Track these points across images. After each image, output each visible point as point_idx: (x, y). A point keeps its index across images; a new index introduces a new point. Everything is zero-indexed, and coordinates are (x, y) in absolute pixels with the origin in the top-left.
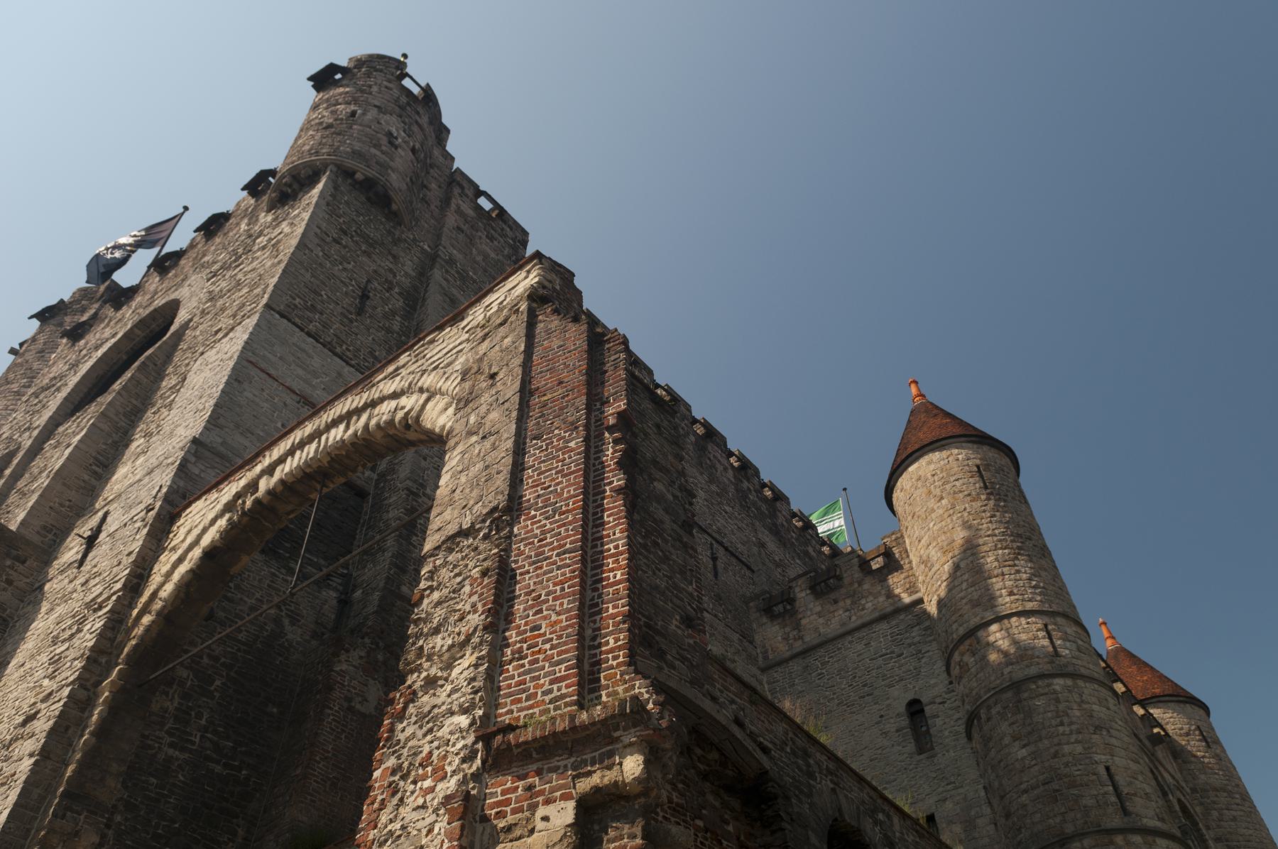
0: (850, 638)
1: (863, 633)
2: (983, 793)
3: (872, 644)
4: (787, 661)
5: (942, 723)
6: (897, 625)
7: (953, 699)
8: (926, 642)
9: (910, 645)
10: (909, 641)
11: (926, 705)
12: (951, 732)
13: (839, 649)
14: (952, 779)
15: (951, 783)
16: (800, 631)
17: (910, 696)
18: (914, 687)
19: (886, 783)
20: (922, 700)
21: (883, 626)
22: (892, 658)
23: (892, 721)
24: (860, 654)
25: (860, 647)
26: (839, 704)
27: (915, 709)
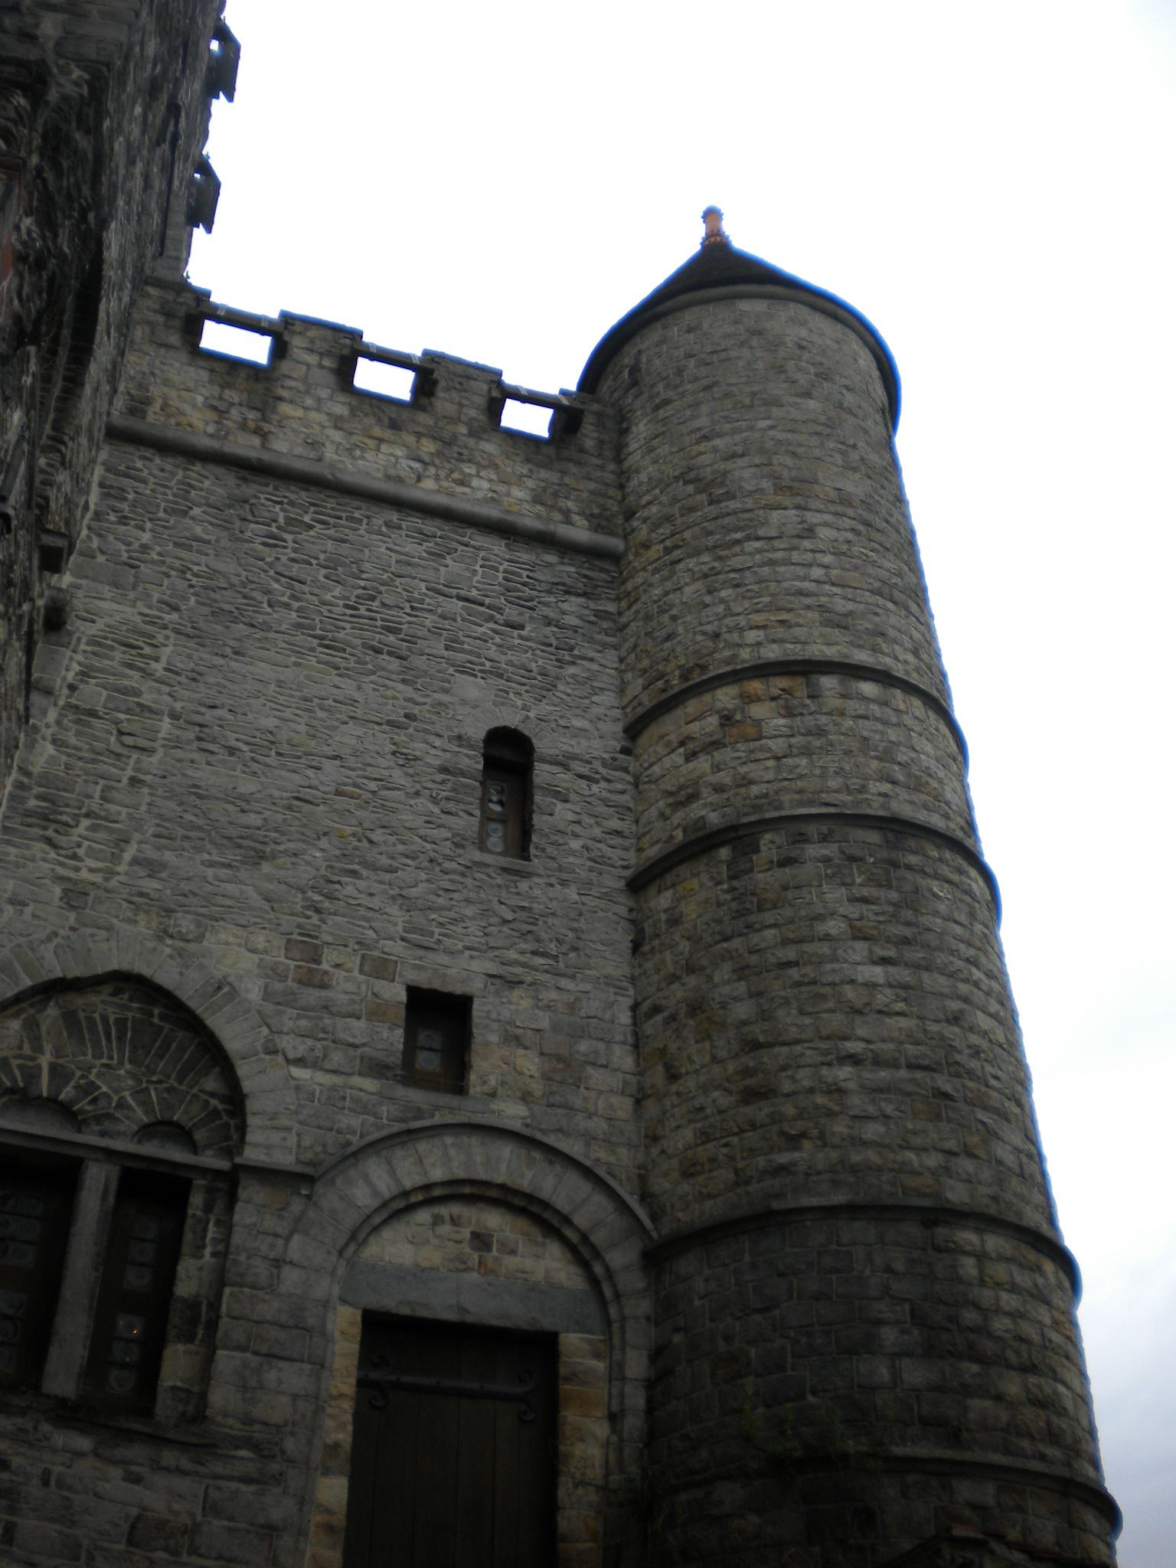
1: (431, 526)
2: (625, 1018)
3: (449, 561)
4: (191, 454)
5: (571, 817)
7: (620, 787)
8: (591, 640)
10: (545, 611)
11: (543, 760)
12: (585, 847)
14: (553, 948)
15: (544, 955)
16: (264, 419)
17: (510, 719)
19: (365, 864)
21: (497, 547)
22: (491, 618)
23: (438, 742)
24: (409, 564)
26: (299, 626)
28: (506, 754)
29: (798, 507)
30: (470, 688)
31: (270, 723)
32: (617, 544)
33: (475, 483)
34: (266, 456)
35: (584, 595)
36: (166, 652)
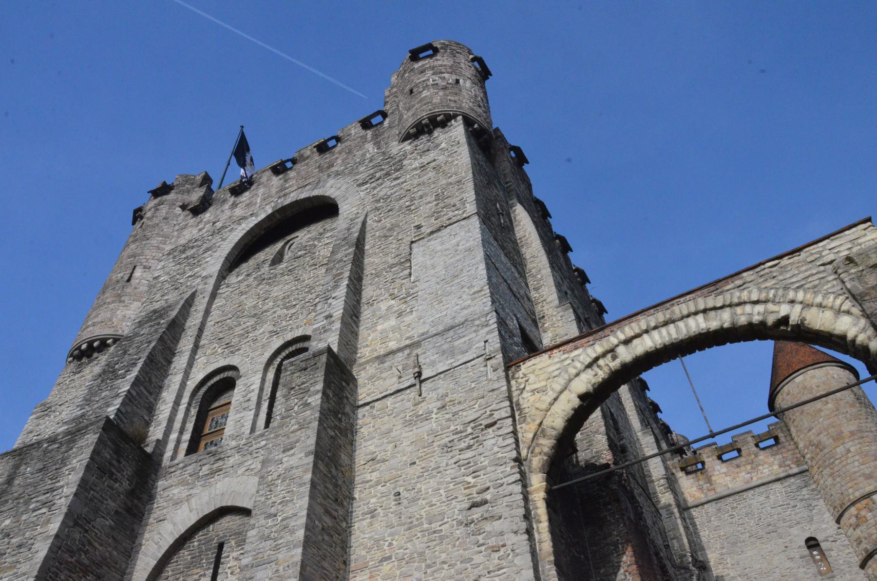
0: (752, 492)
1: (762, 489)
4: (703, 504)
6: (789, 486)
8: (815, 499)
9: (802, 500)
10: (801, 497)
13: (744, 499)
17: (808, 535)
18: (810, 529)
20: (817, 538)
21: (777, 486)
22: (788, 508)
23: (796, 551)
25: (762, 498)
26: (750, 537)
27: (812, 543)
28: (812, 543)
29: (842, 444)
30: (795, 531)
31: (759, 566)
32: (805, 467)
33: (764, 471)
34: (718, 495)
35: (806, 486)
36: (728, 561)
